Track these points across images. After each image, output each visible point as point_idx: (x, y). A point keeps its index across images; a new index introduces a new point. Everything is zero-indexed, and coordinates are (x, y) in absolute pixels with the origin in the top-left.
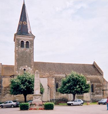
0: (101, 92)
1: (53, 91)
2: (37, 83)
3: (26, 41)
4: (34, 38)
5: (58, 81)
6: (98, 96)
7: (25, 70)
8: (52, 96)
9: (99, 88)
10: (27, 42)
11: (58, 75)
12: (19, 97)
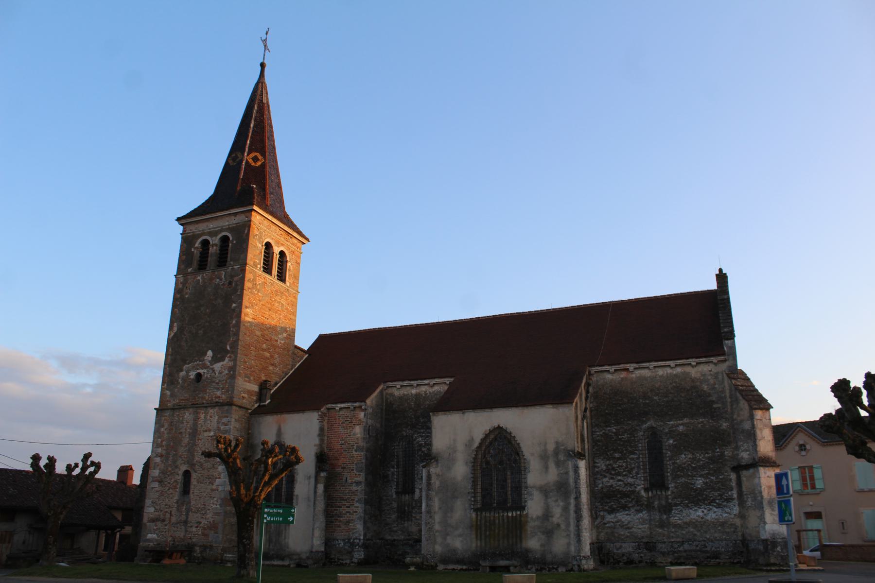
6: (697, 514)
7: (199, 376)
8: (348, 522)
11: (414, 391)
12: (159, 524)
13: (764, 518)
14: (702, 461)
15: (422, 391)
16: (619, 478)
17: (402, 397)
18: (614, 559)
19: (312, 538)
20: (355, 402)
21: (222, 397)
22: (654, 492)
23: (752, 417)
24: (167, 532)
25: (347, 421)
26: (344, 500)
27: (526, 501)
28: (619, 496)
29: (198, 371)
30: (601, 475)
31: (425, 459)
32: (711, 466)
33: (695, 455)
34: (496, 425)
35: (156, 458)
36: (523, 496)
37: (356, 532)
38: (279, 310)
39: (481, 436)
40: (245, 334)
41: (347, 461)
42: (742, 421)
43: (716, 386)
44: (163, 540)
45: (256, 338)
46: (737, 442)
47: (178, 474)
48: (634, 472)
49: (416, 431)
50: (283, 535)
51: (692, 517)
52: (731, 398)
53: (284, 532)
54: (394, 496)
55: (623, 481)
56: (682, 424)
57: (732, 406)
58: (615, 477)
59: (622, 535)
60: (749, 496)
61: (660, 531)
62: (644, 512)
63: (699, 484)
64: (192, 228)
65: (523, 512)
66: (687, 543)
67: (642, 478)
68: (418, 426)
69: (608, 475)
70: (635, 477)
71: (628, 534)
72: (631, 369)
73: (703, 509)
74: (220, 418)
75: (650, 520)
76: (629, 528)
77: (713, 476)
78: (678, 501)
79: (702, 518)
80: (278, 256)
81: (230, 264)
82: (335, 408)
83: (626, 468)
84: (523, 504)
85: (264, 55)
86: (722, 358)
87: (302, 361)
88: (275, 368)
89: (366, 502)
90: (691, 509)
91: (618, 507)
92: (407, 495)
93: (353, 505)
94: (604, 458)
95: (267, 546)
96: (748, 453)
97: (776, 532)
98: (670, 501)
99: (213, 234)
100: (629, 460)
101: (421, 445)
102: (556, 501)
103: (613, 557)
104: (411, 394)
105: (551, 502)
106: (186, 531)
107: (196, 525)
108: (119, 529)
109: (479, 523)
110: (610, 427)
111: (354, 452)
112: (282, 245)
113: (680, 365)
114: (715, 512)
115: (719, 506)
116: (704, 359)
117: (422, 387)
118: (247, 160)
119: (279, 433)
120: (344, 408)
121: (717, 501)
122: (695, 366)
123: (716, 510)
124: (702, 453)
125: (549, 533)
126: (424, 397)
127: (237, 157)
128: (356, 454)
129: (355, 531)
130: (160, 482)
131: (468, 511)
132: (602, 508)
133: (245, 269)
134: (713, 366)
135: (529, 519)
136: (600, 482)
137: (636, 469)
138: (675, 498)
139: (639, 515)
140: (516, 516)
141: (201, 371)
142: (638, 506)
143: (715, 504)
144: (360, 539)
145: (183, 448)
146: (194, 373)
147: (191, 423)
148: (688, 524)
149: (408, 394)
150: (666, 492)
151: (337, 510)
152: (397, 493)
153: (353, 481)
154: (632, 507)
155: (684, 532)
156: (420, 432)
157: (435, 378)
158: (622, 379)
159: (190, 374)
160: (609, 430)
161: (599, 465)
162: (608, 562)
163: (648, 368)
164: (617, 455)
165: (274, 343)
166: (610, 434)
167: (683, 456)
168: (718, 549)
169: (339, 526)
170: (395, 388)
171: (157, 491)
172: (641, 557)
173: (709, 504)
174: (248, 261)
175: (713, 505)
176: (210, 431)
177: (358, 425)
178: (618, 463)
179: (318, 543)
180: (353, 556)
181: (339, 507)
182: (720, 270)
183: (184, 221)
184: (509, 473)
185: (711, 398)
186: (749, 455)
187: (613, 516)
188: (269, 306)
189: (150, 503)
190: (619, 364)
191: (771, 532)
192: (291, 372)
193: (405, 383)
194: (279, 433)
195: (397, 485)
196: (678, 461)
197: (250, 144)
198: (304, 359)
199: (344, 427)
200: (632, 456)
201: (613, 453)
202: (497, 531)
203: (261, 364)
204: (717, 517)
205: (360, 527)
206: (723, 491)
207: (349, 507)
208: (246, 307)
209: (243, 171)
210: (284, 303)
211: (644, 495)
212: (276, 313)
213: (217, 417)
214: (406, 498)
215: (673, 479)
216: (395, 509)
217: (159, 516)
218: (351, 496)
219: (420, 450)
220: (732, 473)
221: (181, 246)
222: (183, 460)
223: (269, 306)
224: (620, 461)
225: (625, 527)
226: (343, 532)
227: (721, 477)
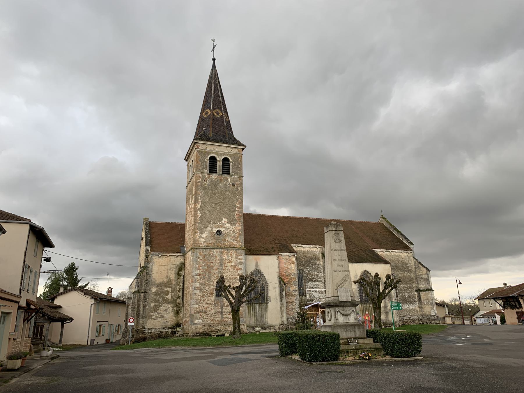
0: (413, 296)
1: (294, 293)
2: (340, 263)
3: (223, 157)
4: (243, 149)
5: (304, 265)
7: (219, 232)
9: (407, 286)
10: (226, 161)
11: (303, 249)
15: (306, 250)
20: (292, 253)
21: (236, 245)
24: (209, 319)
29: (219, 229)
31: (310, 281)
35: (196, 276)
42: (421, 275)
44: (206, 323)
46: (418, 282)
47: (213, 286)
49: (305, 268)
50: (264, 317)
52: (415, 265)
57: (415, 269)
68: (305, 266)
72: (384, 251)
74: (237, 256)
81: (233, 174)
82: (282, 255)
86: (411, 251)
92: (303, 297)
95: (256, 323)
96: (425, 286)
99: (221, 155)
101: (308, 274)
106: (222, 317)
107: (229, 314)
109: (363, 309)
111: (292, 276)
115: (413, 304)
117: (307, 248)
119: (257, 265)
123: (412, 305)
130: (201, 290)
145: (214, 271)
146: (217, 230)
147: (219, 257)
149: (300, 251)
156: (307, 268)
157: (313, 245)
159: (214, 230)
171: (199, 295)
173: (410, 303)
176: (231, 262)
177: (292, 263)
185: (407, 265)
189: (195, 302)
190: (381, 249)
194: (257, 265)
199: (286, 264)
207: (292, 302)
213: (235, 255)
214: (303, 298)
215: (399, 293)
217: (203, 309)
218: (293, 297)
219: (308, 276)
222: (215, 278)
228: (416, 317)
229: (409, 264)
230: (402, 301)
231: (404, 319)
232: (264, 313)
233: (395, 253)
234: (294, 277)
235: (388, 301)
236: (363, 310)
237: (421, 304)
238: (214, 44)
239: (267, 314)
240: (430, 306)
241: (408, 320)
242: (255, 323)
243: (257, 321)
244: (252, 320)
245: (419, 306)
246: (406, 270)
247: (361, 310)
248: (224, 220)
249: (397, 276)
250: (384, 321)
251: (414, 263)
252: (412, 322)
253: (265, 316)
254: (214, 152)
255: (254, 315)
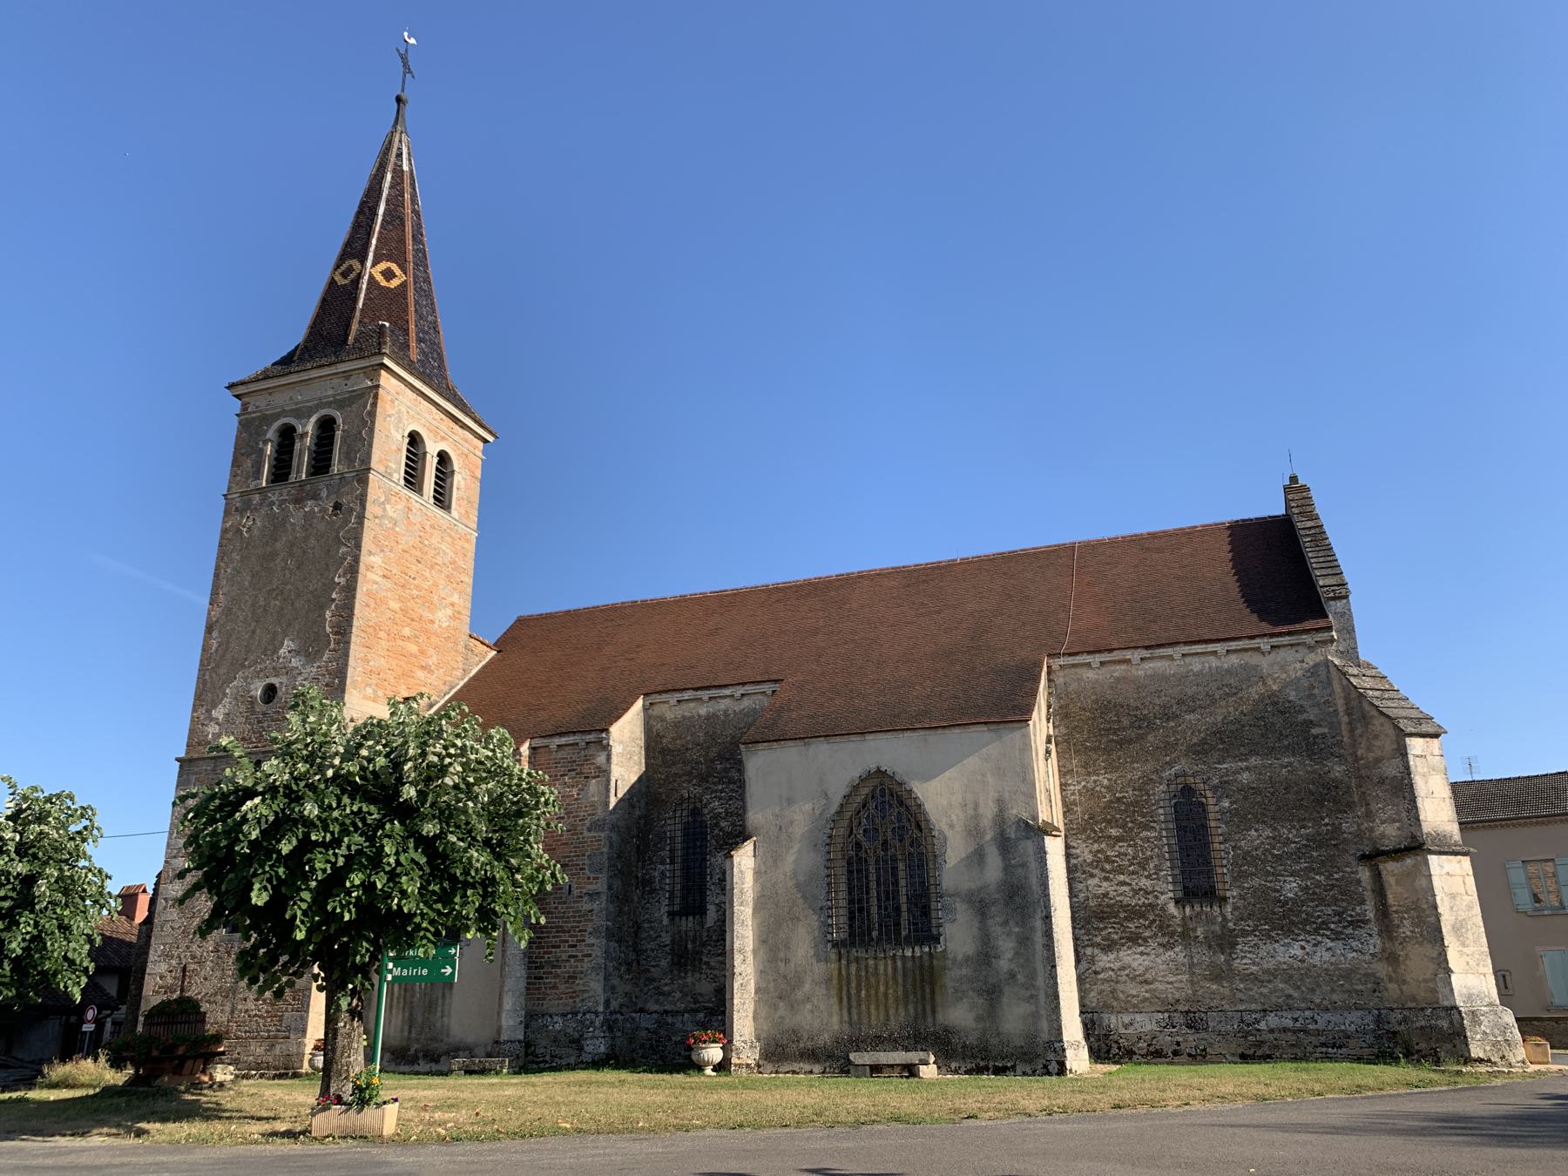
0: (1347, 892)
5: (703, 779)
7: (270, 691)
8: (572, 977)
11: (703, 711)
13: (1446, 961)
14: (1295, 842)
16: (1122, 878)
17: (679, 722)
18: (1119, 1048)
19: (499, 1014)
20: (590, 732)
22: (1197, 908)
23: (1403, 752)
25: (573, 770)
26: (564, 932)
27: (940, 926)
28: (1122, 915)
29: (268, 681)
30: (1084, 872)
31: (727, 844)
32: (1315, 854)
33: (1279, 832)
34: (873, 767)
36: (933, 914)
37: (589, 997)
38: (437, 564)
39: (844, 791)
40: (368, 606)
41: (571, 852)
42: (1378, 760)
43: (1316, 691)
45: (389, 614)
46: (1368, 804)
48: (1152, 865)
50: (439, 1009)
51: (1279, 958)
52: (1349, 713)
53: (440, 1001)
54: (666, 921)
55: (1130, 885)
56: (1247, 768)
57: (1352, 731)
58: (1111, 876)
59: (1134, 997)
60: (1406, 916)
61: (1214, 987)
62: (1177, 949)
63: (1291, 890)
64: (260, 403)
65: (935, 947)
66: (1272, 1015)
67: (1170, 879)
68: (710, 779)
69: (1096, 871)
70: (1154, 876)
71: (1147, 995)
73: (1302, 943)
75: (1192, 965)
76: (1146, 982)
77: (1321, 874)
78: (1248, 925)
79: (1302, 961)
80: (436, 460)
83: (1134, 858)
84: (934, 931)
85: (404, 82)
87: (484, 663)
88: (429, 675)
89: (610, 935)
90: (1277, 941)
91: (1121, 938)
92: (691, 918)
93: (584, 941)
94: (1089, 837)
95: (406, 1033)
97: (1475, 991)
98: (1231, 925)
100: (1140, 842)
102: (1006, 923)
103: (1117, 1042)
104: (699, 716)
105: (996, 929)
108: (109, 1012)
109: (844, 972)
110: (1098, 775)
111: (586, 834)
112: (443, 439)
113: (1235, 651)
114: (1329, 949)
115: (1336, 936)
116: (1287, 638)
118: (371, 277)
120: (566, 745)
121: (1332, 926)
122: (1270, 653)
123: (1330, 944)
124: (1294, 827)
125: (992, 994)
126: (724, 722)
127: (350, 269)
128: (589, 837)
129: (586, 995)
131: (821, 946)
132: (1088, 940)
133: (368, 478)
134: (1306, 651)
135: (949, 962)
136: (1081, 886)
137: (1155, 860)
138: (1242, 919)
139: (1167, 954)
140: (921, 956)
141: (275, 681)
142: (1163, 935)
143: (1328, 933)
144: (596, 1013)
148: (1272, 974)
150: (1220, 907)
151: (551, 953)
152: (671, 914)
153: (584, 891)
154: (1151, 938)
155: (1265, 991)
156: (716, 791)
158: (1118, 680)
160: (1095, 781)
161: (1078, 851)
162: (1108, 1052)
163: (1171, 658)
164: (1114, 832)
165: (429, 626)
166: (1098, 789)
167: (1253, 832)
168: (1343, 1028)
169: (555, 987)
170: (666, 705)
172: (1178, 1044)
173: (1316, 932)
174: (373, 465)
175: (1323, 935)
177: (595, 777)
178: (1117, 848)
179: (511, 1023)
180: (581, 1049)
181: (553, 947)
182: (1294, 479)
183: (241, 390)
184: (901, 866)
185: (1301, 718)
186: (1399, 829)
187: (1112, 956)
188: (418, 553)
191: (1464, 991)
192: (462, 684)
193: (687, 695)
195: (672, 898)
196: (1243, 843)
197: (376, 246)
198: (487, 660)
200: (1145, 833)
201: (1105, 827)
202: (882, 988)
203: (401, 666)
204: (1333, 960)
205: (596, 986)
206: (1344, 904)
207: (575, 946)
208: (370, 553)
209: (362, 296)
210: (448, 551)
211: (1176, 913)
212: (432, 568)
214: (688, 924)
215: (1235, 879)
216: (667, 949)
218: (580, 922)
219: (717, 825)
220: (1360, 868)
221: (237, 438)
223: (418, 553)
224: (1121, 844)
225: (1138, 979)
226: (561, 999)
227: (1336, 876)
228: (1355, 1016)
229: (1316, 711)
230: (1259, 920)
231: (1263, 1025)
232: (440, 995)
233: (1212, 658)
234: (593, 834)
235: (1006, 923)
236: (848, 975)
237: (1391, 938)
238: (400, 54)
239: (451, 997)
240: (1430, 946)
241: (1295, 1032)
242: (402, 1031)
243: (410, 1027)
244: (393, 1022)
245: (1384, 950)
246: (1287, 747)
247: (830, 979)
248: (288, 644)
249: (1226, 782)
250: (972, 1040)
251: (1345, 698)
252: (1323, 1045)
253: (443, 1004)
254: (288, 411)
255: (402, 1000)
